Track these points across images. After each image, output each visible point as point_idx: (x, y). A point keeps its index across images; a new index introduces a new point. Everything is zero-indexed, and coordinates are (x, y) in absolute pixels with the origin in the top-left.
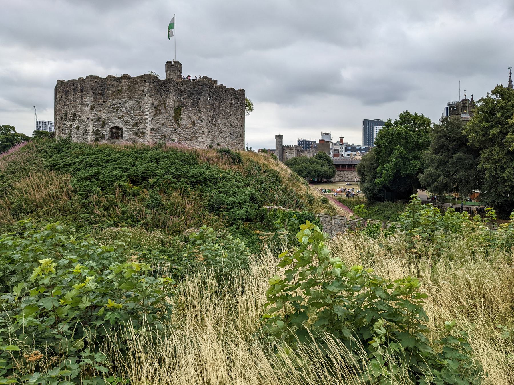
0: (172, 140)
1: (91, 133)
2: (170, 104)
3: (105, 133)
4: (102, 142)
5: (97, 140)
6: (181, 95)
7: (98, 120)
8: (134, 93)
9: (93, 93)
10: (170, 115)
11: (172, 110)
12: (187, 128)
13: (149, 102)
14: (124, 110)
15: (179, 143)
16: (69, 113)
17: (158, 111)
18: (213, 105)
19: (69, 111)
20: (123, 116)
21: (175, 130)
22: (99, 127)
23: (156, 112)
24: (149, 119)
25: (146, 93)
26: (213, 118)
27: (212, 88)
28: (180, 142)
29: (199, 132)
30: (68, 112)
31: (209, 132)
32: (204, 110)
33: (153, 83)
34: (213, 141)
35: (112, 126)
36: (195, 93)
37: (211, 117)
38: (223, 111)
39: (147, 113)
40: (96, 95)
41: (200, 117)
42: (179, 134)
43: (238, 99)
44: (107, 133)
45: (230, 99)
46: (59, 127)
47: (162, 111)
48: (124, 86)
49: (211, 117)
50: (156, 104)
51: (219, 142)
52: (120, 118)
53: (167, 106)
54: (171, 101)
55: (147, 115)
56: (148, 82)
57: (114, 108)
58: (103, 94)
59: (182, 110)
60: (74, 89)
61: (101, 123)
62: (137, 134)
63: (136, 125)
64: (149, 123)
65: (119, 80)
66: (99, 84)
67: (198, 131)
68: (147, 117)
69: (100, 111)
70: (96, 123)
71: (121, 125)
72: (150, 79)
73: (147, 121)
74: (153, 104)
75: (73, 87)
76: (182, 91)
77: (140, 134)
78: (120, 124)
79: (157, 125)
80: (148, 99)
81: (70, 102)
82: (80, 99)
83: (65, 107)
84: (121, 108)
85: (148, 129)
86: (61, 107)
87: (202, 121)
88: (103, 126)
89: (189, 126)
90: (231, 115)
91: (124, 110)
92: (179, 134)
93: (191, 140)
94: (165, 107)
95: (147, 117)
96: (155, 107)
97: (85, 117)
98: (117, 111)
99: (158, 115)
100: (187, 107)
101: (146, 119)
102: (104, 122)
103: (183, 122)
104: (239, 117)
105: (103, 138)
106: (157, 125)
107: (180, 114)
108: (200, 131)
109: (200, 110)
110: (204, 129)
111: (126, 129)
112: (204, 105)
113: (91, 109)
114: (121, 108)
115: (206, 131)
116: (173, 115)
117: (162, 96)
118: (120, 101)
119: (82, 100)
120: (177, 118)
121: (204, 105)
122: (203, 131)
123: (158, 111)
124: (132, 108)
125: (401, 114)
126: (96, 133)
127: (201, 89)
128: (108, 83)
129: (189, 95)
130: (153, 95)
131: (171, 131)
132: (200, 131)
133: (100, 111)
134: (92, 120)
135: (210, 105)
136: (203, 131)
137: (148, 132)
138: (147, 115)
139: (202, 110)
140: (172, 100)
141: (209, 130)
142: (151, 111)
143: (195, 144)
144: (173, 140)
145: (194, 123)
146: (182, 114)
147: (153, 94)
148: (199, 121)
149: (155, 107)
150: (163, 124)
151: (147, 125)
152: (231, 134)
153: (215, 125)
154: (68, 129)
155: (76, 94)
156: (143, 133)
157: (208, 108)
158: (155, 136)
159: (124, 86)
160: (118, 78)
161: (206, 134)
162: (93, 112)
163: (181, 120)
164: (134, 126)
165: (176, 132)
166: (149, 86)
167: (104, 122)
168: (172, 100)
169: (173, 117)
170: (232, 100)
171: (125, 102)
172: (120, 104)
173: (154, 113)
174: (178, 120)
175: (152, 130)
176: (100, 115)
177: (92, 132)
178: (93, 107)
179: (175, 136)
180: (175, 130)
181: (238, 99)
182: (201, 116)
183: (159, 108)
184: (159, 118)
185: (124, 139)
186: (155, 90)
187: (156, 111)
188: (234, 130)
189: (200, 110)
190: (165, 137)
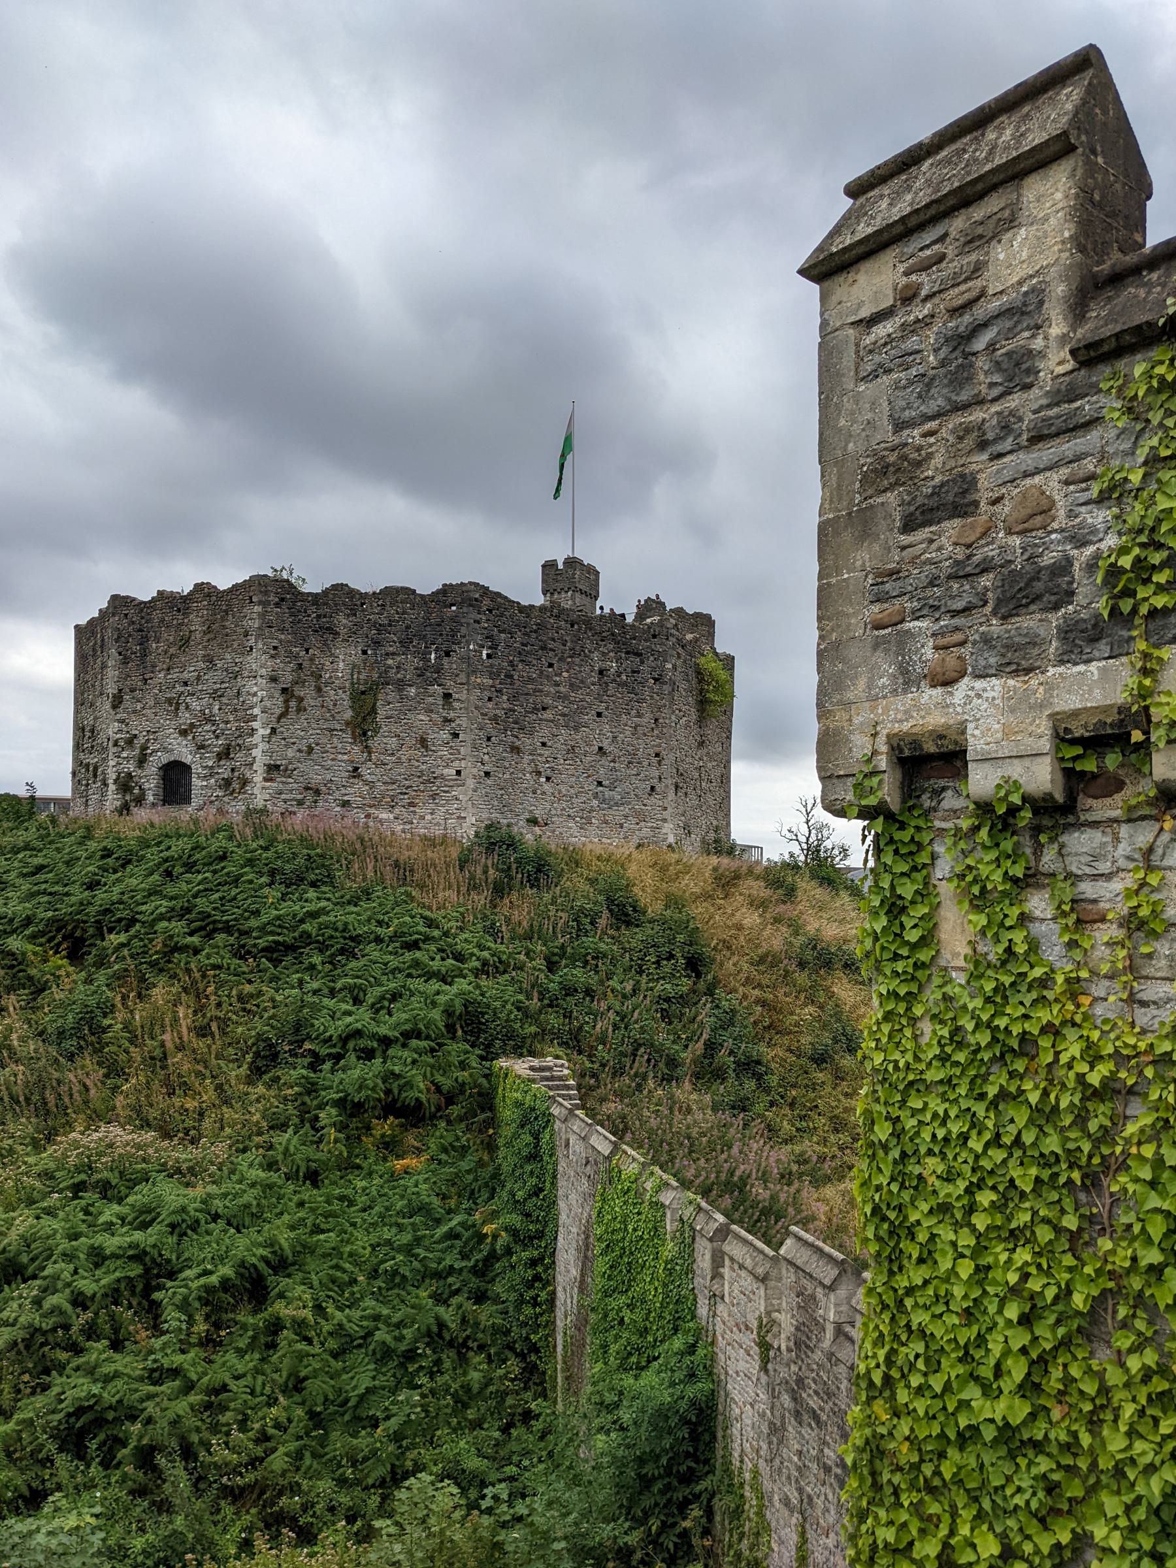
1: (112, 787)
2: (337, 678)
3: (147, 786)
4: (142, 815)
5: (125, 809)
6: (377, 643)
7: (130, 742)
8: (220, 645)
11: (345, 699)
12: (399, 762)
13: (263, 671)
15: (368, 816)
17: (293, 704)
20: (192, 725)
22: (131, 767)
23: (287, 708)
24: (261, 732)
25: (252, 642)
27: (502, 615)
28: (372, 811)
29: (442, 776)
31: (487, 774)
32: (463, 696)
34: (505, 807)
35: (165, 758)
37: (495, 719)
39: (256, 711)
40: (125, 661)
41: (447, 721)
42: (366, 783)
44: (150, 782)
45: (596, 656)
47: (309, 701)
48: (196, 623)
49: (495, 719)
50: (287, 678)
51: (538, 813)
52: (184, 733)
53: (327, 684)
54: (341, 665)
55: (254, 718)
56: (260, 603)
57: (169, 701)
58: (144, 655)
59: (380, 696)
61: (137, 751)
62: (227, 783)
63: (225, 754)
64: (262, 746)
67: (438, 772)
68: (255, 725)
69: (135, 712)
70: (124, 754)
71: (187, 759)
72: (266, 593)
73: (257, 739)
74: (274, 679)
77: (234, 785)
79: (290, 753)
80: (258, 662)
85: (259, 767)
87: (456, 735)
88: (142, 761)
89: (404, 754)
91: (195, 705)
92: (366, 783)
93: (412, 804)
94: (319, 690)
95: (255, 725)
96: (284, 690)
98: (177, 709)
99: (292, 715)
100: (401, 685)
101: (253, 731)
102: (144, 748)
103: (384, 740)
105: (140, 800)
106: (290, 753)
107: (374, 711)
108: (446, 771)
109: (447, 696)
110: (463, 764)
112: (462, 678)
113: (114, 707)
115: (471, 770)
116: (348, 715)
117: (307, 651)
118: (185, 675)
121: (462, 678)
122: (458, 773)
123: (293, 704)
124: (216, 695)
125: (705, 623)
126: (125, 784)
127: (452, 619)
128: (156, 616)
129: (405, 643)
130: (275, 648)
131: (341, 773)
132: (446, 771)
133: (135, 712)
134: (116, 744)
135: (492, 675)
137: (258, 778)
138: (254, 718)
139: (455, 696)
141: (487, 768)
142: (268, 704)
143: (428, 817)
144: (345, 804)
145: (423, 742)
146: (382, 712)
147: (275, 643)
148: (445, 735)
149: (284, 690)
150: (310, 750)
151: (255, 752)
153: (515, 750)
156: (245, 782)
157: (481, 687)
159: (196, 623)
161: (471, 783)
162: (118, 717)
163: (376, 732)
164: (220, 756)
165: (359, 776)
166: (262, 615)
167: (144, 748)
169: (348, 724)
171: (198, 678)
172: (186, 684)
173: (278, 712)
174: (365, 734)
175: (272, 769)
176: (138, 726)
177: (116, 781)
178: (117, 702)
179: (355, 791)
180: (356, 769)
182: (452, 715)
183: (299, 691)
184: (295, 728)
185: (196, 802)
187: (286, 701)
188: (614, 769)
189: (447, 696)
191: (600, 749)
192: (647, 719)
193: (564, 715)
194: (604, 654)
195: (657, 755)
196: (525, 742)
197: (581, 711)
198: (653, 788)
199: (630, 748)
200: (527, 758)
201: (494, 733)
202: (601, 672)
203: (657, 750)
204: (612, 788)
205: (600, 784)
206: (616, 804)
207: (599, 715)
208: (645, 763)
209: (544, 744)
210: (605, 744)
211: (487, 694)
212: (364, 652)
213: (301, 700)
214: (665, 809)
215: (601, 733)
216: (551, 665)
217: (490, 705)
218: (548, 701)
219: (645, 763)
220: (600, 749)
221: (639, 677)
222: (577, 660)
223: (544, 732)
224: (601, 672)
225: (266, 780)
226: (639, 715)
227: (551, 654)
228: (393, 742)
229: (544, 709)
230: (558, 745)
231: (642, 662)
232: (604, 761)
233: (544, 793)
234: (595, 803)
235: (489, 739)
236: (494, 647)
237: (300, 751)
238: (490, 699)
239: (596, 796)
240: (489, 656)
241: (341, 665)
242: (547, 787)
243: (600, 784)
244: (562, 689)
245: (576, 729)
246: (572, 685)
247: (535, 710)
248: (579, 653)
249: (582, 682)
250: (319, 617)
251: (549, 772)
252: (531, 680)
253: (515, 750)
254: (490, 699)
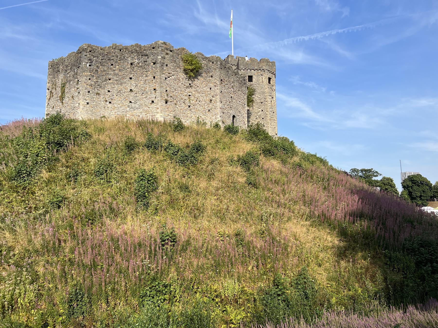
18: (97, 71)
27: (95, 52)
37: (91, 85)
49: (91, 85)
191: (131, 90)
192: (151, 77)
193: (116, 80)
194: (132, 58)
195: (155, 89)
196: (102, 91)
197: (123, 78)
198: (153, 102)
199: (143, 89)
200: (102, 96)
201: (91, 90)
202: (131, 64)
203: (154, 87)
204: (135, 103)
205: (131, 102)
206: (137, 109)
207: (131, 78)
208: (149, 93)
209: (109, 91)
210: (133, 88)
211: (89, 78)
214: (158, 108)
215: (131, 85)
216: (112, 65)
217: (89, 81)
218: (110, 77)
219: (149, 93)
220: (131, 90)
221: (147, 63)
222: (122, 61)
223: (109, 87)
224: (131, 64)
226: (146, 76)
227: (112, 61)
229: (110, 79)
230: (114, 91)
231: (148, 58)
232: (133, 94)
233: (108, 107)
234: (128, 109)
235: (89, 92)
236: (91, 62)
238: (90, 79)
239: (129, 106)
240: (90, 65)
242: (109, 105)
243: (131, 102)
244: (116, 72)
245: (121, 84)
246: (120, 70)
247: (106, 80)
248: (123, 59)
249: (124, 68)
251: (110, 101)
252: (104, 71)
253: (98, 94)
254: (90, 79)
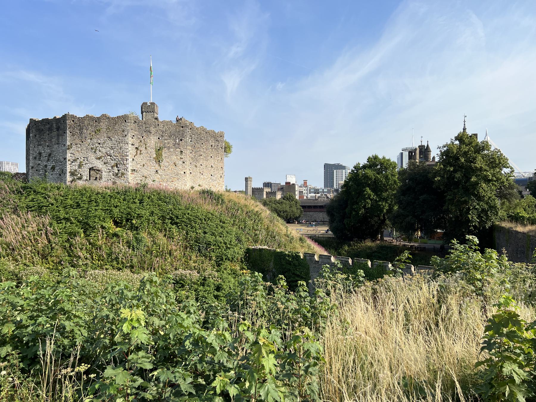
0: (153, 181)
2: (151, 145)
9: (71, 132)
10: (151, 156)
14: (104, 150)
16: (44, 153)
17: (139, 152)
19: (44, 150)
21: (157, 171)
26: (195, 160)
28: (162, 183)
30: (43, 151)
33: (134, 123)
36: (176, 134)
38: (204, 152)
43: (218, 141)
46: (32, 168)
50: (137, 145)
53: (148, 147)
54: (152, 141)
59: (163, 151)
60: (49, 128)
65: (98, 120)
66: (76, 123)
75: (48, 126)
76: (163, 132)
78: (99, 164)
79: (138, 166)
81: (45, 141)
82: (56, 138)
83: (39, 146)
84: (101, 149)
86: (35, 147)
90: (211, 157)
96: (137, 148)
97: (61, 158)
104: (220, 158)
111: (106, 170)
114: (101, 149)
116: (155, 156)
117: (143, 137)
119: (58, 139)
120: (158, 160)
123: (139, 152)
130: (133, 136)
136: (185, 173)
140: (153, 141)
146: (164, 155)
148: (181, 163)
149: (137, 148)
150: (144, 165)
152: (212, 175)
154: (42, 169)
155: (51, 133)
158: (135, 177)
160: (97, 118)
168: (153, 141)
170: (212, 142)
173: (135, 154)
174: (159, 161)
180: (157, 171)
181: (218, 141)
184: (138, 158)
186: (135, 131)
190: (146, 177)
212: (159, 138)
213: (141, 151)
225: (131, 174)
228: (167, 164)
237: (141, 165)
241: (152, 141)
250: (146, 128)
